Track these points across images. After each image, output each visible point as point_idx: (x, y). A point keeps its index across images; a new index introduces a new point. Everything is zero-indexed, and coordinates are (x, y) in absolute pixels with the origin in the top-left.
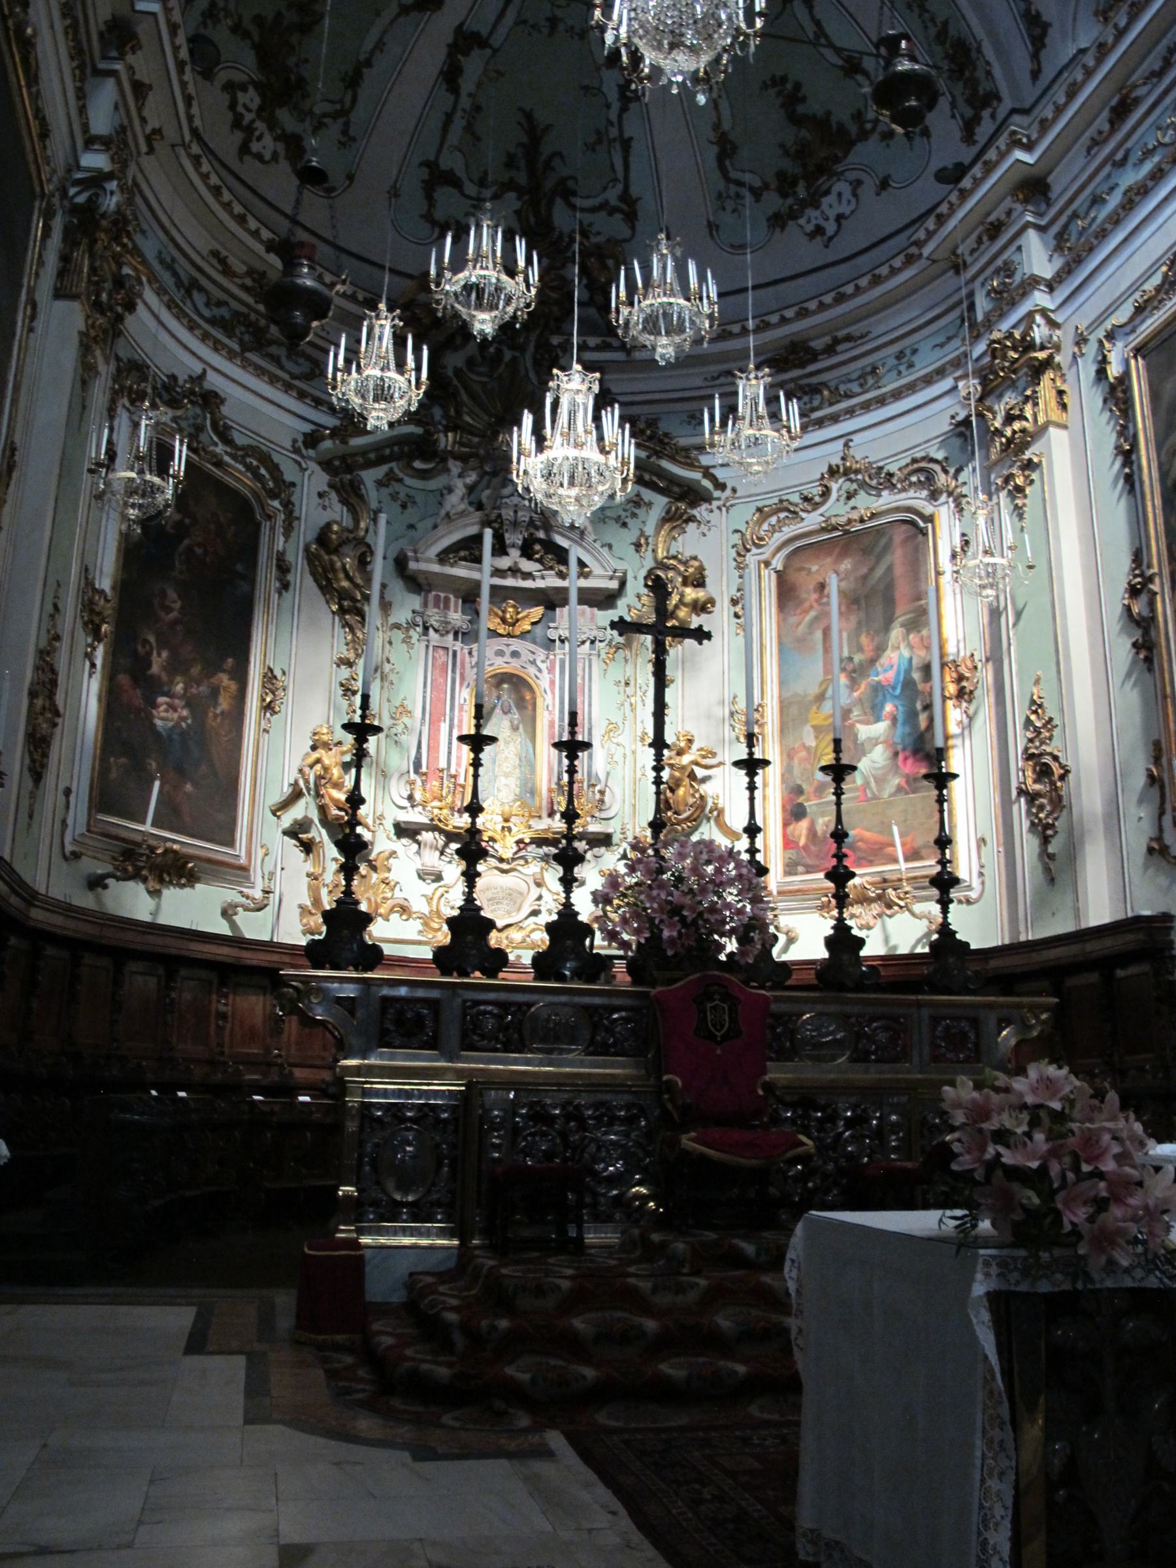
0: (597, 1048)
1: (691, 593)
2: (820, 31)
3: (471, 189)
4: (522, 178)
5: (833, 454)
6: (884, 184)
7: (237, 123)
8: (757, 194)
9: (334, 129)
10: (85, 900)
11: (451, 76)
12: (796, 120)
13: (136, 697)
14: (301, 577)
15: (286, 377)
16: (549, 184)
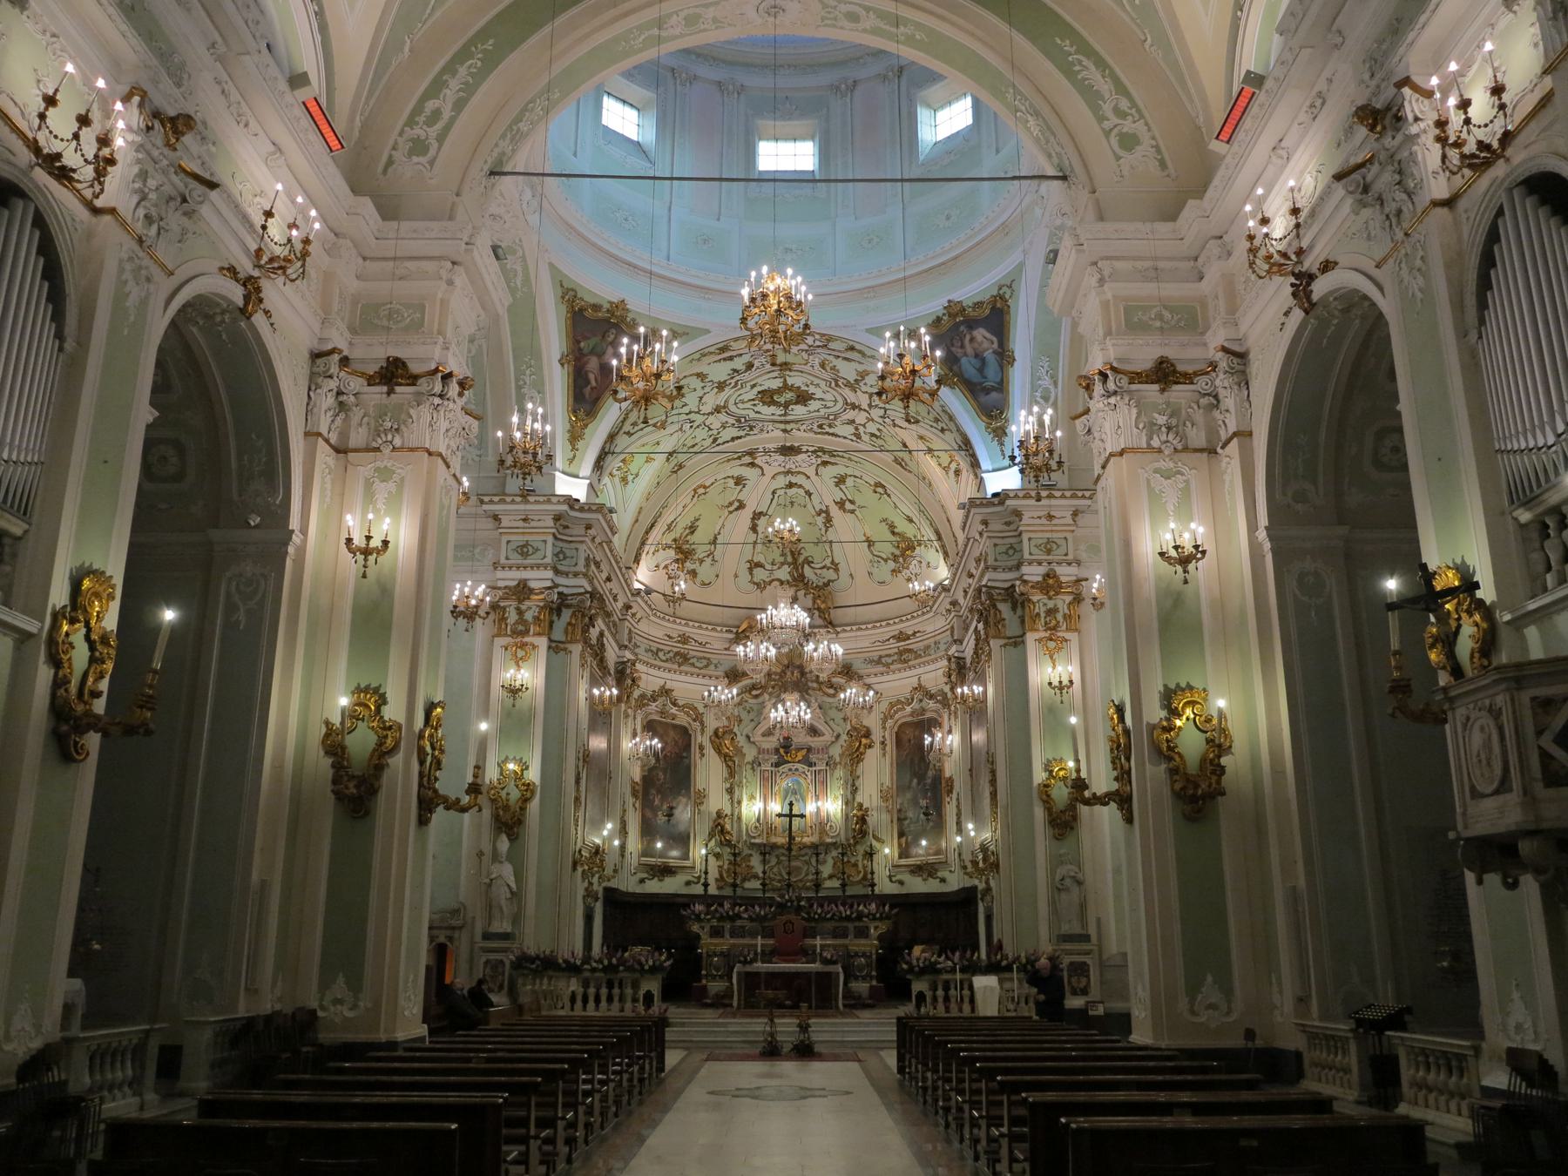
1: (864, 741)
2: (896, 507)
4: (790, 559)
8: (886, 560)
9: (709, 560)
11: (754, 528)
12: (893, 533)
13: (649, 814)
14: (710, 751)
16: (801, 559)
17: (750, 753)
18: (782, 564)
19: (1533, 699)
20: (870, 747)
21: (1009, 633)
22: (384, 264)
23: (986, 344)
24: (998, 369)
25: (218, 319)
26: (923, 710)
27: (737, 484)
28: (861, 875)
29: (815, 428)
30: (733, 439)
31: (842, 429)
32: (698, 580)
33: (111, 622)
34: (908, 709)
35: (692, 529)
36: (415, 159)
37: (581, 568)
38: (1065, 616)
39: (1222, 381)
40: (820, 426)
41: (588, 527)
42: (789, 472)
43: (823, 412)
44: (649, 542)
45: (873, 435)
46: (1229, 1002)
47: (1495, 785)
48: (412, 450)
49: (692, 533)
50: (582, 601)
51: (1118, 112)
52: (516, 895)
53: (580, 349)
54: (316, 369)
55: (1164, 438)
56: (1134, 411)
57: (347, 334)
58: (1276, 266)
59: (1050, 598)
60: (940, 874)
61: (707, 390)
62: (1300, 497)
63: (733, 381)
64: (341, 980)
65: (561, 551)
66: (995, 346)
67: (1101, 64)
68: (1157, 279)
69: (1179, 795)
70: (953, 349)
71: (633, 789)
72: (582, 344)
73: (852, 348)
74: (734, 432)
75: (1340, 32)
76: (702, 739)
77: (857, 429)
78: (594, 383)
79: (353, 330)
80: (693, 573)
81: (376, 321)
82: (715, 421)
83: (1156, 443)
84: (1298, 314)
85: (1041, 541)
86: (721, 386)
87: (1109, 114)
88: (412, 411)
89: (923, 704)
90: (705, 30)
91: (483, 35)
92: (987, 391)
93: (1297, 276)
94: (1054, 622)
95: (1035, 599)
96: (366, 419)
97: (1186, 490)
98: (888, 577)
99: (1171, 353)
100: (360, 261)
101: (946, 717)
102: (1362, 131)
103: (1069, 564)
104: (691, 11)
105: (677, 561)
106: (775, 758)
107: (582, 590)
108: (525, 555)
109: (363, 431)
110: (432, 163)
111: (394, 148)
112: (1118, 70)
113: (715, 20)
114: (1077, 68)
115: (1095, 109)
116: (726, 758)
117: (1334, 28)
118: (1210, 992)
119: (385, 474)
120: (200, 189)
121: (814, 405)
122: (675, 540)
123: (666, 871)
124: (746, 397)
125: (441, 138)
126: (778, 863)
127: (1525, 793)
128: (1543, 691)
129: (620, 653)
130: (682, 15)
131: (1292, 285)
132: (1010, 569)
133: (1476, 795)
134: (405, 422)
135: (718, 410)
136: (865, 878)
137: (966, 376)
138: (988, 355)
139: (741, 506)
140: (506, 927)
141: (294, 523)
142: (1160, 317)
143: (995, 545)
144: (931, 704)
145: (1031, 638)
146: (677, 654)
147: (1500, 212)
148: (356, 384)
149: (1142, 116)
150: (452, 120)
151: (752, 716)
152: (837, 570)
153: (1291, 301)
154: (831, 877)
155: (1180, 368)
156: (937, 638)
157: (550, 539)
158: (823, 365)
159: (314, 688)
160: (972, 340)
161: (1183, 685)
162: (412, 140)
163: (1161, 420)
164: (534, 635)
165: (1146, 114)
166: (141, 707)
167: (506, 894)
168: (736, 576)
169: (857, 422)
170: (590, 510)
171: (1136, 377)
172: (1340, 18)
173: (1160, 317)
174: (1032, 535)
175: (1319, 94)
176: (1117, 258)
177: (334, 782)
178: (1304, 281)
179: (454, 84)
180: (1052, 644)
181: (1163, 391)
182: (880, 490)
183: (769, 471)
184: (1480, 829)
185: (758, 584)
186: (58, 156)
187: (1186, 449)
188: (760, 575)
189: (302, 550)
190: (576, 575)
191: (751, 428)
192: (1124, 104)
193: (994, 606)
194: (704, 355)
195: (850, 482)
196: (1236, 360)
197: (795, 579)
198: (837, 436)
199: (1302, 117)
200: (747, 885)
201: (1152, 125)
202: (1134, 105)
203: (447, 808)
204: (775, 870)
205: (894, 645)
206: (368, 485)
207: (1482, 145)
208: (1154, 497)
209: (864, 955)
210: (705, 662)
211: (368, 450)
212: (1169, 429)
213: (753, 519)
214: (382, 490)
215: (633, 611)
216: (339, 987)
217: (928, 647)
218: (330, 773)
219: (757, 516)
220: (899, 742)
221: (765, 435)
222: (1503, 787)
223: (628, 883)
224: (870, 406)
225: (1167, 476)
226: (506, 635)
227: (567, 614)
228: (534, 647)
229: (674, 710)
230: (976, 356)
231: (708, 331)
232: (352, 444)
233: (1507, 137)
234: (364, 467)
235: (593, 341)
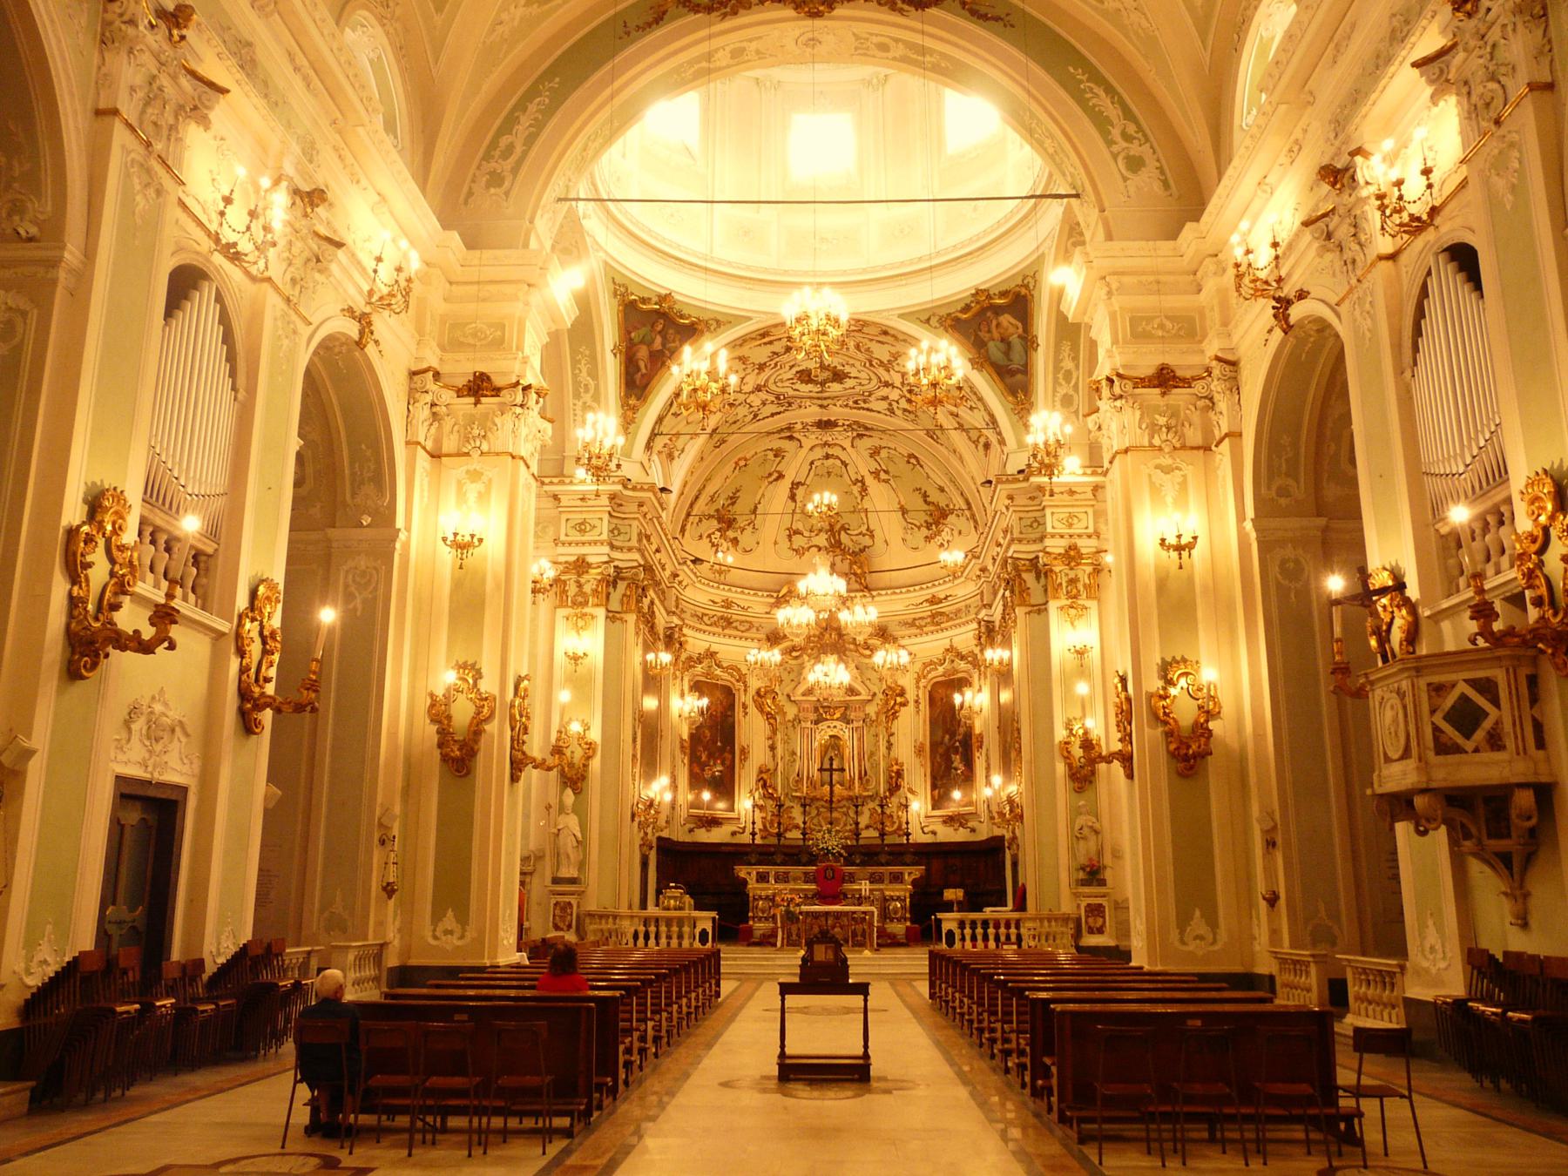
0: (806, 882)
2: (928, 477)
3: (806, 534)
5: (946, 644)
6: (960, 533)
7: (713, 545)
8: (919, 528)
9: (750, 529)
10: (688, 839)
11: (793, 497)
14: (752, 709)
15: (739, 633)
16: (837, 527)
17: (791, 711)
18: (820, 531)
19: (1429, 685)
20: (904, 704)
21: (1033, 601)
22: (468, 288)
23: (1011, 330)
24: (1023, 353)
25: (336, 350)
26: (957, 671)
27: (776, 456)
28: (896, 826)
29: (851, 403)
30: (773, 415)
31: (875, 405)
32: (739, 547)
33: (276, 622)
34: (941, 669)
35: (733, 499)
36: (492, 190)
37: (634, 543)
38: (1085, 585)
39: (1216, 386)
40: (856, 402)
41: (641, 505)
42: (826, 444)
43: (858, 389)
44: (694, 513)
45: (905, 410)
46: (1215, 934)
47: (1400, 752)
48: (497, 454)
49: (733, 504)
50: (636, 574)
51: (1127, 138)
52: (581, 844)
53: (631, 339)
54: (413, 386)
55: (1164, 437)
56: (1138, 413)
57: (438, 351)
58: (1261, 289)
59: (1072, 569)
60: (970, 824)
61: (749, 371)
62: (1283, 492)
63: (773, 363)
64: (450, 913)
65: (616, 528)
66: (1020, 330)
67: (1109, 90)
68: (1159, 292)
69: (1173, 755)
70: (981, 334)
71: (682, 747)
72: (633, 335)
73: (885, 333)
74: (774, 409)
75: (1311, 93)
76: (745, 698)
77: (890, 404)
78: (644, 371)
79: (443, 348)
80: (735, 541)
81: (461, 339)
82: (756, 400)
83: (1157, 442)
84: (1278, 334)
85: (1062, 516)
86: (762, 367)
87: (1119, 139)
88: (497, 420)
89: (955, 664)
92: (1012, 373)
93: (1278, 300)
94: (1075, 591)
95: (1057, 569)
96: (456, 428)
97: (1183, 485)
98: (922, 543)
99: (1171, 360)
101: (976, 676)
102: (1326, 188)
103: (1089, 536)
104: (738, 45)
105: (719, 530)
106: (813, 716)
107: (635, 564)
108: (583, 532)
109: (455, 437)
110: (507, 194)
112: (1125, 96)
113: (758, 52)
114: (1089, 95)
115: (1105, 134)
116: (769, 716)
117: (1306, 88)
118: (1198, 925)
119: (475, 476)
120: (332, 248)
121: (849, 383)
122: (717, 511)
123: (713, 822)
124: (786, 376)
125: (515, 171)
126: (818, 814)
127: (1420, 760)
128: (1436, 679)
129: (668, 619)
130: (728, 49)
131: (1274, 308)
132: (1035, 541)
133: (1388, 760)
134: (490, 429)
135: (758, 389)
136: (899, 828)
137: (993, 359)
138: (1014, 339)
139: (781, 476)
140: (573, 873)
141: (400, 523)
142: (1161, 326)
143: (1020, 519)
144: (962, 665)
145: (1053, 606)
146: (722, 618)
147: (1429, 273)
148: (448, 396)
149: (1147, 140)
150: (525, 154)
151: (792, 676)
152: (872, 537)
153: (1273, 322)
154: (867, 827)
155: (1179, 373)
156: (968, 602)
157: (606, 517)
158: (858, 347)
159: (420, 668)
160: (998, 325)
161: (1178, 658)
163: (1162, 421)
164: (594, 605)
166: (308, 689)
167: (571, 842)
168: (776, 543)
169: (891, 397)
170: (642, 489)
171: (1141, 382)
172: (1310, 82)
173: (1161, 326)
174: (1055, 510)
175: (1296, 142)
176: (1123, 273)
177: (440, 745)
178: (1283, 304)
179: (525, 121)
180: (1072, 611)
181: (1164, 394)
182: (913, 461)
183: (807, 443)
184: (1390, 786)
185: (796, 551)
186: (235, 245)
187: (1183, 447)
188: (799, 541)
189: (406, 546)
190: (630, 549)
191: (790, 404)
192: (1132, 129)
193: (1020, 576)
194: (745, 341)
195: (884, 453)
196: (1228, 368)
197: (832, 546)
198: (872, 410)
199: (1283, 159)
200: (789, 835)
202: (1140, 129)
203: (535, 767)
204: (815, 821)
205: (927, 609)
206: (460, 485)
207: (1413, 218)
208: (1156, 490)
209: (898, 899)
210: (747, 625)
211: (459, 454)
212: (1169, 429)
213: (792, 489)
214: (473, 490)
215: (680, 578)
216: (449, 921)
217: (959, 610)
218: (436, 739)
219: (795, 485)
220: (932, 701)
221: (803, 411)
222: (1406, 754)
223: (680, 835)
224: (903, 383)
225: (1167, 470)
226: (567, 606)
227: (622, 586)
228: (593, 617)
229: (718, 672)
230: (1002, 340)
231: (749, 319)
232: (445, 450)
233: (1434, 211)
234: (456, 470)
235: (644, 331)
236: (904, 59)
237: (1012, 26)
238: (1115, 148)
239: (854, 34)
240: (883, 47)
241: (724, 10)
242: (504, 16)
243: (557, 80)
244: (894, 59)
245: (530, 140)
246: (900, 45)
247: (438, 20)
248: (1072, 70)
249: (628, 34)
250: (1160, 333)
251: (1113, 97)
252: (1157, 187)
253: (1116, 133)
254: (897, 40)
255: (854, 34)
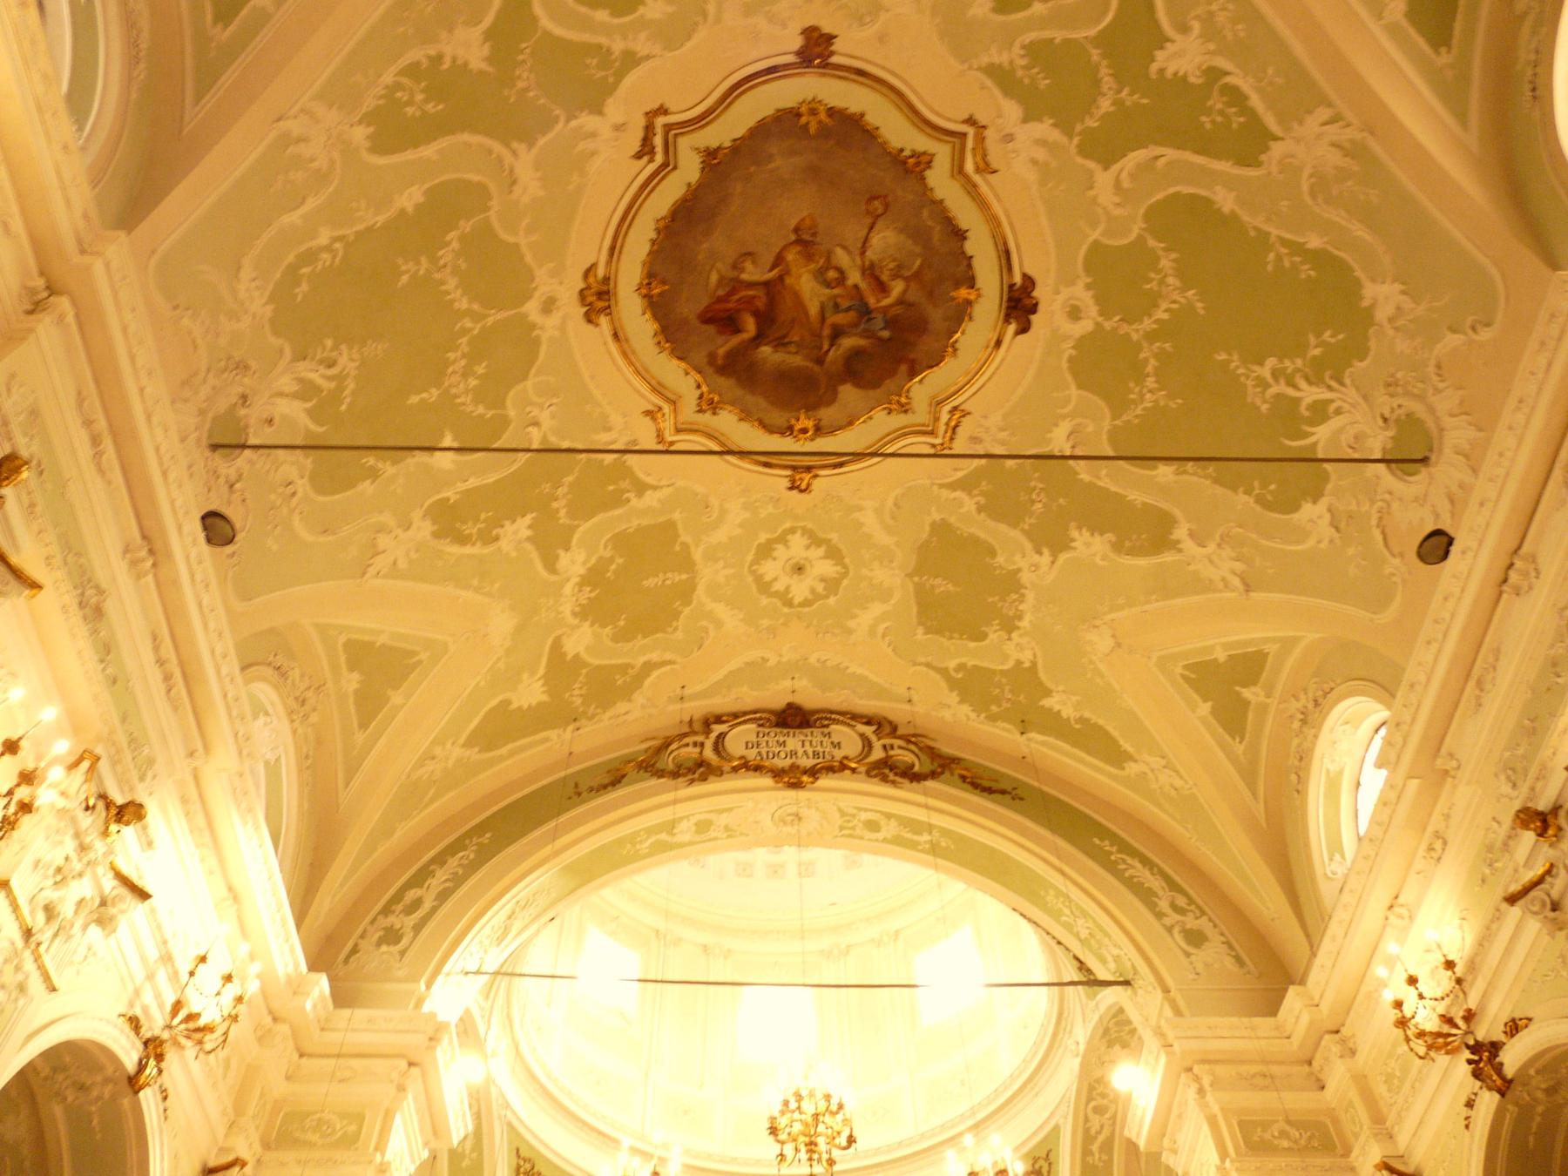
22: (324, 1062)
36: (384, 948)
57: (257, 1147)
58: (1438, 1042)
67: (1145, 861)
75: (1451, 755)
79: (266, 1146)
87: (1168, 911)
90: (716, 839)
91: (480, 829)
100: (296, 1056)
102: (1529, 837)
104: (702, 817)
110: (402, 953)
111: (362, 937)
117: (1444, 751)
125: (418, 928)
130: (694, 820)
142: (1283, 1134)
149: (1203, 913)
150: (434, 910)
162: (385, 929)
165: (1206, 909)
172: (1448, 739)
175: (1437, 835)
176: (1216, 1062)
192: (1181, 901)
199: (1419, 864)
201: (1217, 921)
202: (1191, 901)
236: (898, 841)
237: (1021, 799)
238: (1167, 921)
239: (840, 810)
240: (872, 826)
241: (690, 777)
242: (438, 751)
243: (488, 835)
244: (885, 840)
245: (443, 896)
246: (893, 823)
247: (360, 738)
248: (1097, 841)
249: (579, 794)
250: (1285, 1144)
251: (1151, 869)
252: (1229, 963)
253: (1164, 905)
254: (889, 816)
255: (840, 810)
